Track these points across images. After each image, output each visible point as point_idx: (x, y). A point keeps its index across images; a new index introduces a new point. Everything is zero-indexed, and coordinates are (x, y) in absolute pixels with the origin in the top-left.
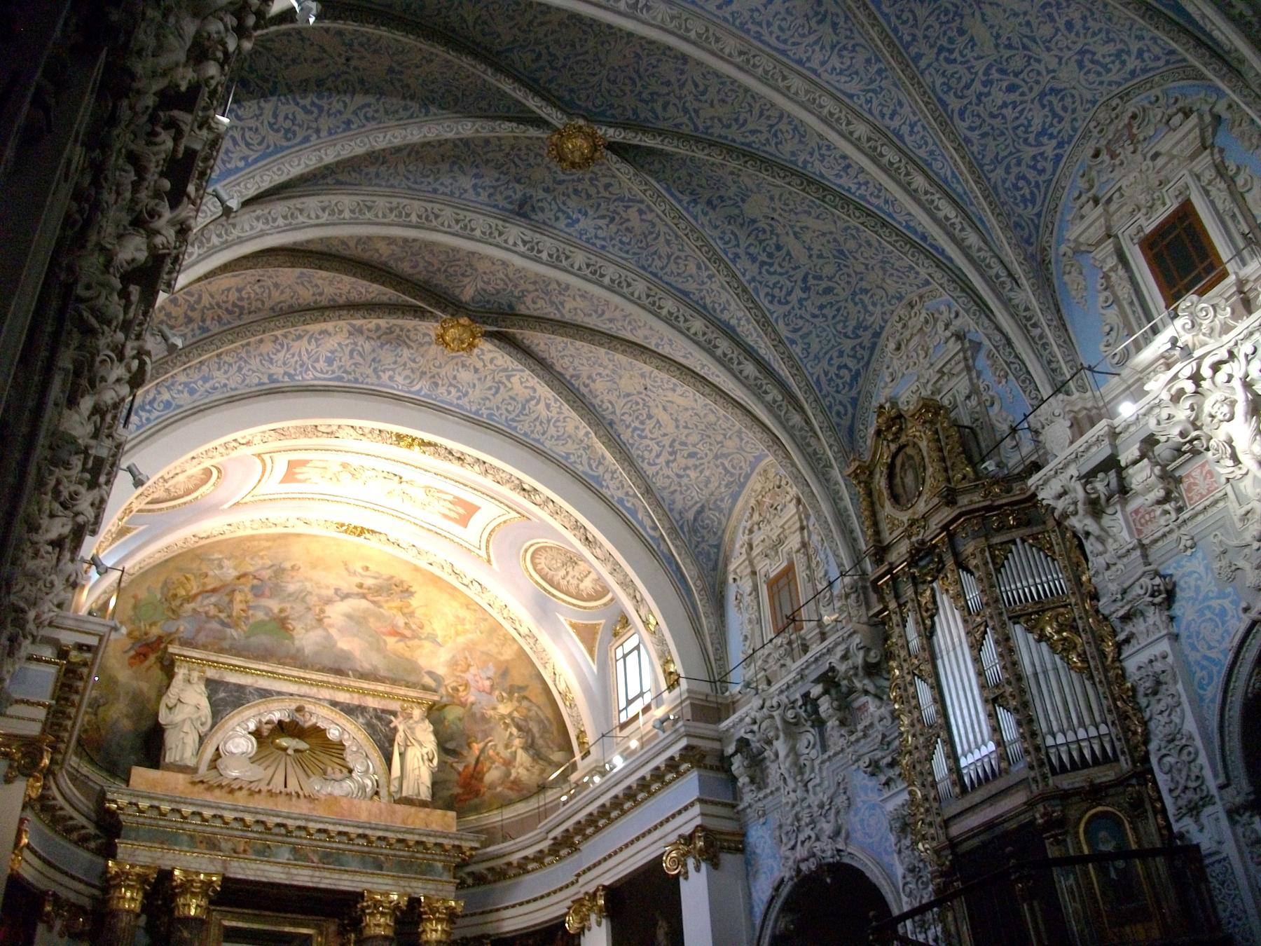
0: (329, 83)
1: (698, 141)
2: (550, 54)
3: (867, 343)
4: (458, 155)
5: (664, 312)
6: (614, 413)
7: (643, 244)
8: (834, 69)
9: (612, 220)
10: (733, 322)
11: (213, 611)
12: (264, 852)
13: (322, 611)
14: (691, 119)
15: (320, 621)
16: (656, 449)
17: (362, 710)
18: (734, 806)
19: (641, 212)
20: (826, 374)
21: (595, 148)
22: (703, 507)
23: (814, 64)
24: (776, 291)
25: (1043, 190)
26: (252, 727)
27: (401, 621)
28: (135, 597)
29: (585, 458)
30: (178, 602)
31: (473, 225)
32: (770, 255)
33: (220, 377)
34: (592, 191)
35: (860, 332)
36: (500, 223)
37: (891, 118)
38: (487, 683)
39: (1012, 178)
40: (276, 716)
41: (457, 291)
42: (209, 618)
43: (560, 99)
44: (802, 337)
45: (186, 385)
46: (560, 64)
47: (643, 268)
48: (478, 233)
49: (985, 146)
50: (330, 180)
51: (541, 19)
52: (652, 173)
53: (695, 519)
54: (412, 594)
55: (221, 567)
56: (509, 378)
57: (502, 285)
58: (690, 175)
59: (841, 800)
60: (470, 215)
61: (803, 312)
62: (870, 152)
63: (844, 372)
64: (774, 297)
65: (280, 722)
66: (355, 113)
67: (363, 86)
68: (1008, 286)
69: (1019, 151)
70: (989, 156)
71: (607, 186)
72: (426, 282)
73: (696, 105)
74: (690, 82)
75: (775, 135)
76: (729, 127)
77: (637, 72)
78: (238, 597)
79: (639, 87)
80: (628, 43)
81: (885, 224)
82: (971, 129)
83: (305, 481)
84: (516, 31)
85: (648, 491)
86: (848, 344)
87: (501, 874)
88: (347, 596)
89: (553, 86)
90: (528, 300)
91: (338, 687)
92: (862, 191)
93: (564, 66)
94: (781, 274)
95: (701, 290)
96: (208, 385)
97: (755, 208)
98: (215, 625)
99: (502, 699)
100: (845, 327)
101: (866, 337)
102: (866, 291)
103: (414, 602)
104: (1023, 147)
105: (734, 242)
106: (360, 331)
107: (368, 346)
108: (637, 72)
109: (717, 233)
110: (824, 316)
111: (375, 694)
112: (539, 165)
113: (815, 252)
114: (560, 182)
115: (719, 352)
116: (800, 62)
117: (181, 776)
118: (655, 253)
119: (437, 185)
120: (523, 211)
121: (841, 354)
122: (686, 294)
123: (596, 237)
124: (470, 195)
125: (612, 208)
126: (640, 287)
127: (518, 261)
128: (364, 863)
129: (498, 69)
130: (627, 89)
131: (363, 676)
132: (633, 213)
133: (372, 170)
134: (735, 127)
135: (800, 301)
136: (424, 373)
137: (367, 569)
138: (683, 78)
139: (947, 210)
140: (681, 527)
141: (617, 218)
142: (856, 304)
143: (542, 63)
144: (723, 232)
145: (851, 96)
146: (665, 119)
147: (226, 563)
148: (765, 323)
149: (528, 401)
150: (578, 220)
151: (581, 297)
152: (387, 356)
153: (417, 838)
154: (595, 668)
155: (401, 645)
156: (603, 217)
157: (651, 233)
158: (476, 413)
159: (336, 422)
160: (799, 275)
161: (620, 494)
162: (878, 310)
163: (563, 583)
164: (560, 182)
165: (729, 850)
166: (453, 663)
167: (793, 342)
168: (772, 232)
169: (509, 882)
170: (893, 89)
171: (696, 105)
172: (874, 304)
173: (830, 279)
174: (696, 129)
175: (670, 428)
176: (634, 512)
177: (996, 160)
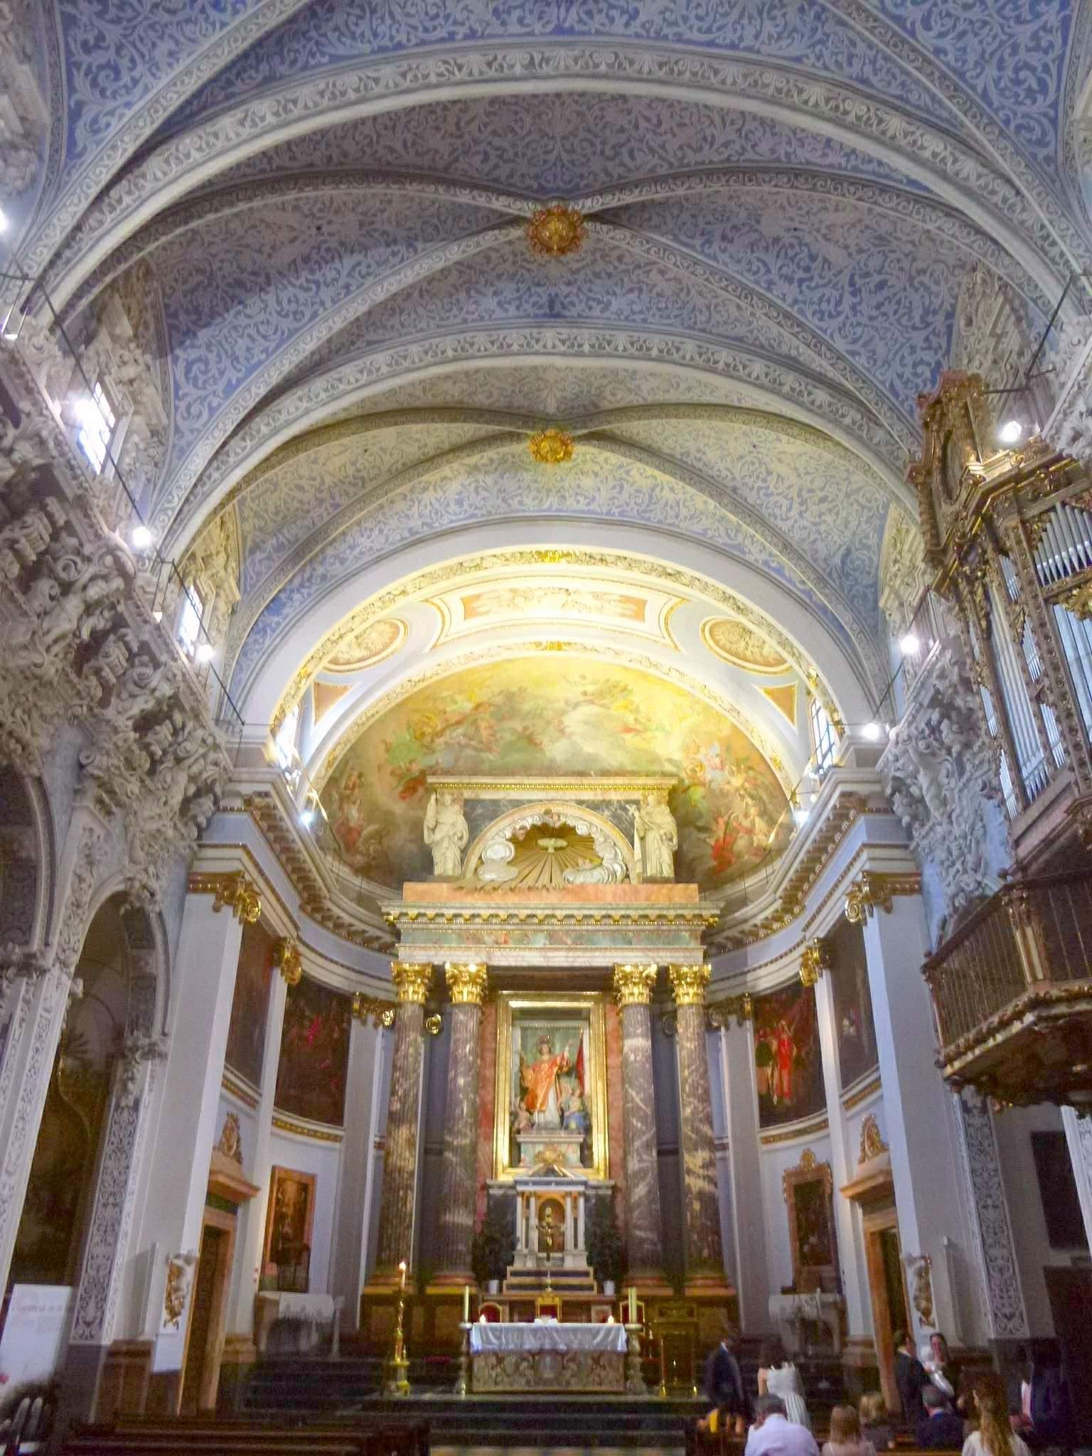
0: (314, 256)
1: (675, 177)
3: (941, 328)
4: (467, 278)
5: (721, 365)
6: (734, 479)
8: (770, 37)
9: (641, 290)
10: (794, 353)
11: (463, 741)
12: (524, 940)
13: (561, 722)
15: (562, 731)
16: (785, 503)
17: (607, 803)
18: (906, 847)
20: (900, 376)
21: (573, 226)
22: (848, 552)
23: (749, 41)
24: (824, 306)
25: (1054, 71)
26: (509, 835)
27: (630, 719)
28: (384, 742)
29: (722, 530)
30: (427, 740)
31: (509, 340)
32: (807, 269)
33: (364, 542)
34: (610, 269)
35: (930, 319)
36: (535, 331)
37: (850, 64)
38: (717, 761)
39: (1009, 73)
40: (528, 823)
41: (541, 407)
42: (462, 747)
43: (529, 188)
44: (865, 345)
45: (336, 557)
46: (511, 154)
47: (690, 327)
48: (515, 348)
49: (964, 50)
50: (359, 344)
51: (467, 117)
52: (657, 228)
53: (843, 563)
54: (631, 692)
55: (455, 702)
56: (627, 473)
57: (577, 390)
58: (693, 216)
59: (979, 832)
60: (502, 333)
61: (859, 318)
62: (832, 114)
63: (919, 369)
64: (822, 312)
65: (534, 826)
66: (349, 275)
67: (347, 248)
68: (1018, 209)
69: (1011, 36)
70: (972, 58)
71: (620, 259)
72: (509, 407)
73: (660, 140)
76: (701, 148)
77: (589, 130)
78: (483, 725)
79: (599, 147)
81: (884, 189)
82: (941, 35)
83: (487, 613)
84: (449, 140)
85: (786, 547)
86: (918, 338)
87: (754, 934)
88: (576, 705)
89: (516, 180)
90: (607, 394)
91: (581, 787)
92: (853, 162)
94: (825, 285)
96: (356, 552)
97: (772, 225)
98: (469, 752)
99: (732, 773)
100: (911, 318)
101: (939, 321)
102: (923, 272)
103: (636, 698)
104: (1018, 29)
105: (763, 270)
106: (476, 468)
107: (489, 480)
109: (743, 265)
110: (884, 314)
111: (616, 788)
113: (853, 249)
114: (577, 271)
115: (786, 389)
116: (733, 46)
117: (445, 886)
119: (463, 315)
120: (554, 312)
121: (913, 349)
122: (739, 339)
123: (633, 313)
124: (499, 313)
125: (634, 278)
126: (690, 347)
127: (559, 362)
128: (614, 940)
129: (452, 183)
130: (589, 151)
131: (605, 773)
132: (654, 275)
133: (395, 321)
134: (706, 147)
135: (853, 308)
136: (549, 490)
137: (584, 677)
139: (933, 144)
140: (830, 574)
142: (917, 290)
143: (493, 160)
144: (750, 263)
145: (798, 59)
147: (458, 698)
148: (817, 343)
149: (653, 490)
150: (610, 303)
151: (653, 379)
152: (509, 483)
153: (657, 912)
154: (795, 728)
155: (637, 739)
156: (631, 290)
158: (609, 513)
159: (477, 555)
160: (844, 279)
161: (764, 556)
162: (943, 289)
163: (748, 653)
164: (577, 271)
165: (904, 892)
166: (686, 749)
167: (854, 354)
168: (800, 244)
169: (761, 943)
171: (660, 140)
172: (937, 283)
173: (879, 272)
174: (671, 165)
175: (793, 479)
176: (779, 571)
177: (981, 62)
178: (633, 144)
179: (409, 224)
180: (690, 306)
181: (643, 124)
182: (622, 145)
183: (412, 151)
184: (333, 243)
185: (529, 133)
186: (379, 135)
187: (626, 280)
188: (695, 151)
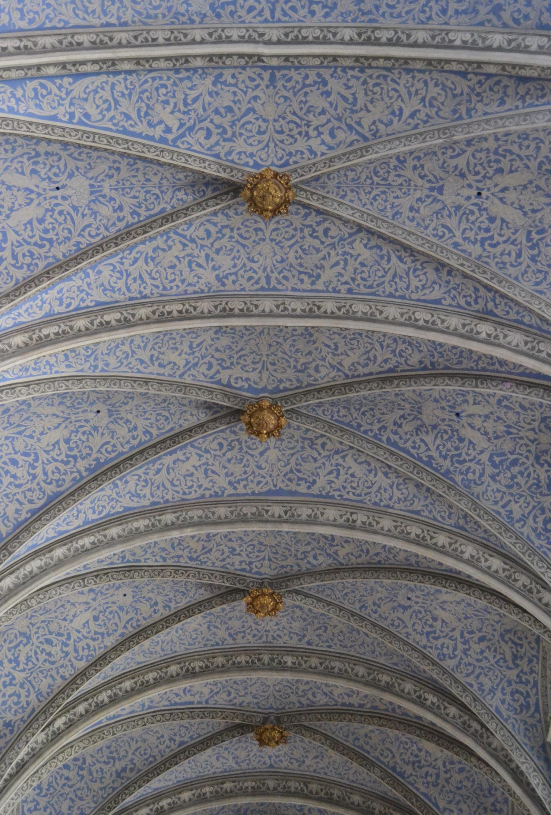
2: (317, 237)
7: (144, 96)
9: (186, 104)
10: (19, 93)
14: (184, 237)
19: (168, 130)
34: (217, 120)
46: (307, 231)
51: (339, 268)
58: (148, 180)
73: (188, 250)
74: (205, 264)
75: (121, 272)
76: (154, 250)
77: (244, 246)
80: (265, 270)
84: (355, 253)
93: (302, 230)
95: (68, 94)
108: (244, 246)
112: (275, 120)
118: (130, 95)
123: (189, 78)
134: (151, 254)
138: (211, 264)
141: (183, 108)
143: (320, 229)
146: (202, 224)
157: (147, 114)
164: (248, 111)
168: (49, 178)
170: (80, 367)
171: (188, 250)
178: (207, 243)
179: (400, 180)
180: (134, 98)
181: (202, 261)
182: (218, 238)
183: (385, 252)
184: (471, 179)
185: (291, 247)
186: (407, 274)
187: (201, 111)
188: (158, 247)
